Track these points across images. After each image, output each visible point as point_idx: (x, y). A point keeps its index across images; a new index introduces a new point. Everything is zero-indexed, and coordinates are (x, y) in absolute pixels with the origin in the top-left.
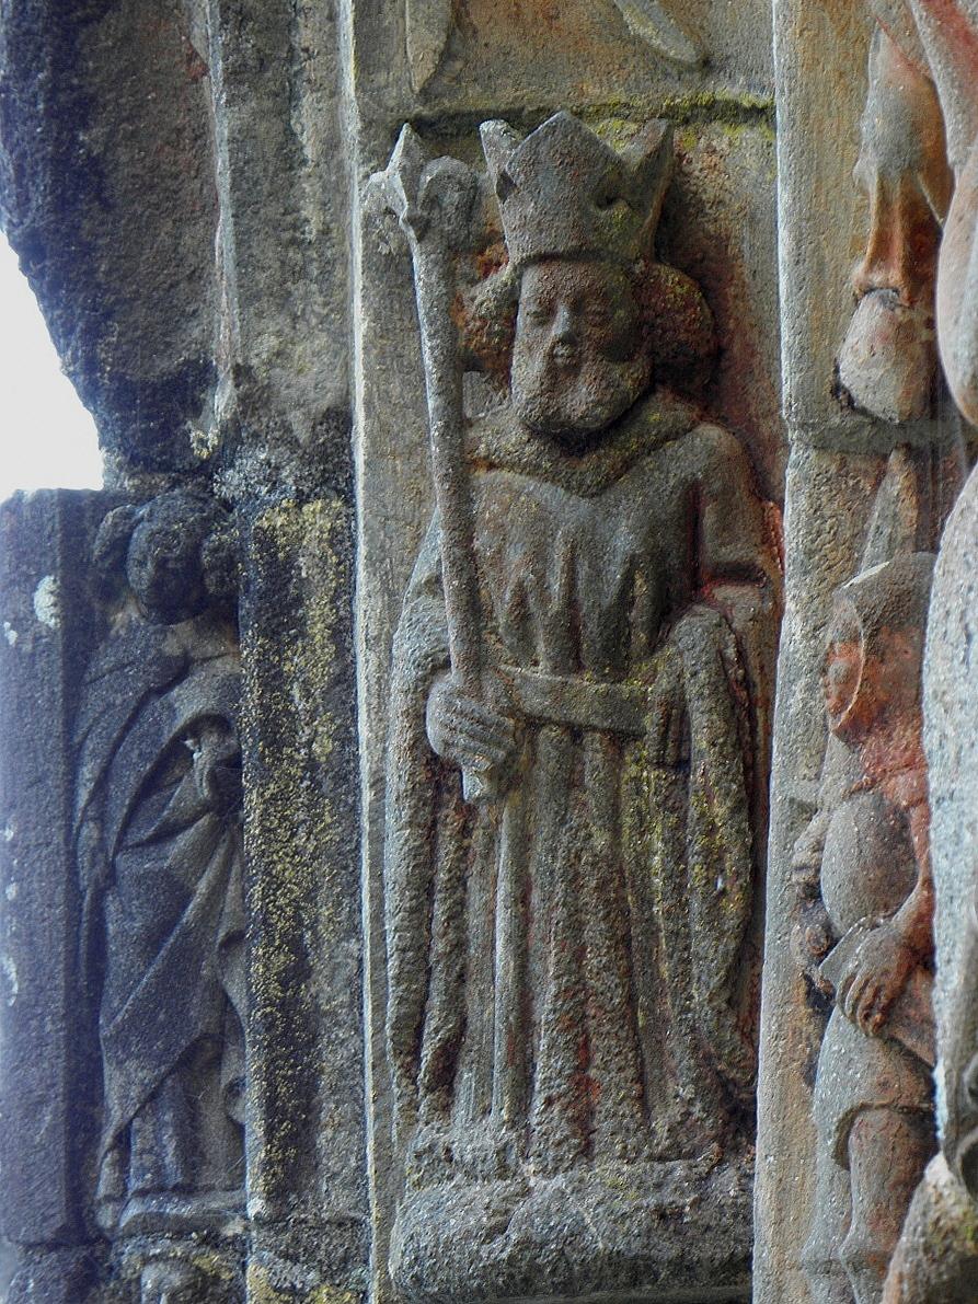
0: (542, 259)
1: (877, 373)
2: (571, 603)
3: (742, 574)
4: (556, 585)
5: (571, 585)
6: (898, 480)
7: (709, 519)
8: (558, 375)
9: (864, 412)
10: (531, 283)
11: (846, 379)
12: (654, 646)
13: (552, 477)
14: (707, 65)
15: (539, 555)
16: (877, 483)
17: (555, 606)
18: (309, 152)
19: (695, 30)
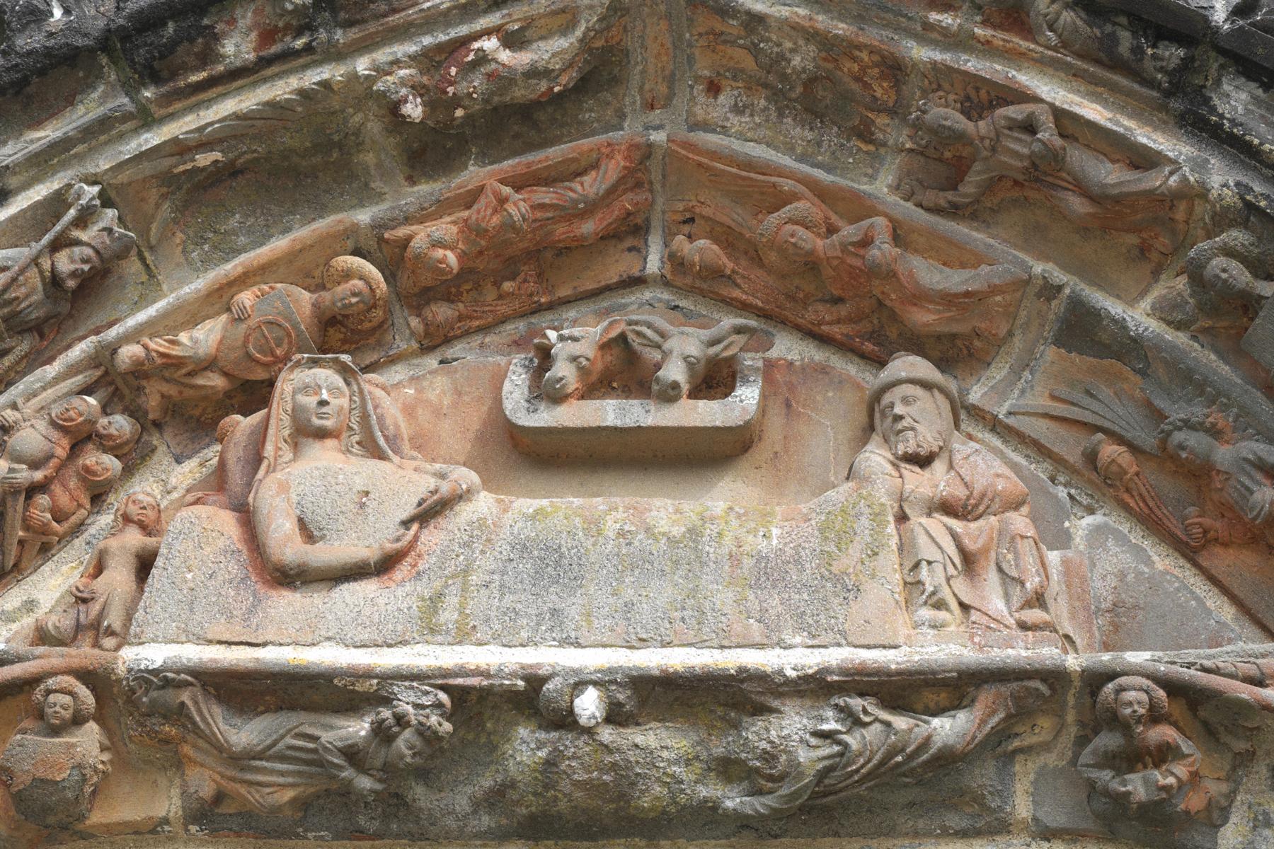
0: (97, 252)
1: (127, 360)
2: (21, 312)
3: (42, 336)
4: (23, 305)
5: (25, 309)
6: (98, 373)
7: (52, 321)
8: (73, 274)
9: (112, 358)
10: (89, 252)
11: (120, 350)
12: (19, 333)
13: (44, 284)
14: (151, 248)
15: (27, 296)
16: (95, 367)
17: (18, 309)
18: (72, 152)
19: (159, 241)
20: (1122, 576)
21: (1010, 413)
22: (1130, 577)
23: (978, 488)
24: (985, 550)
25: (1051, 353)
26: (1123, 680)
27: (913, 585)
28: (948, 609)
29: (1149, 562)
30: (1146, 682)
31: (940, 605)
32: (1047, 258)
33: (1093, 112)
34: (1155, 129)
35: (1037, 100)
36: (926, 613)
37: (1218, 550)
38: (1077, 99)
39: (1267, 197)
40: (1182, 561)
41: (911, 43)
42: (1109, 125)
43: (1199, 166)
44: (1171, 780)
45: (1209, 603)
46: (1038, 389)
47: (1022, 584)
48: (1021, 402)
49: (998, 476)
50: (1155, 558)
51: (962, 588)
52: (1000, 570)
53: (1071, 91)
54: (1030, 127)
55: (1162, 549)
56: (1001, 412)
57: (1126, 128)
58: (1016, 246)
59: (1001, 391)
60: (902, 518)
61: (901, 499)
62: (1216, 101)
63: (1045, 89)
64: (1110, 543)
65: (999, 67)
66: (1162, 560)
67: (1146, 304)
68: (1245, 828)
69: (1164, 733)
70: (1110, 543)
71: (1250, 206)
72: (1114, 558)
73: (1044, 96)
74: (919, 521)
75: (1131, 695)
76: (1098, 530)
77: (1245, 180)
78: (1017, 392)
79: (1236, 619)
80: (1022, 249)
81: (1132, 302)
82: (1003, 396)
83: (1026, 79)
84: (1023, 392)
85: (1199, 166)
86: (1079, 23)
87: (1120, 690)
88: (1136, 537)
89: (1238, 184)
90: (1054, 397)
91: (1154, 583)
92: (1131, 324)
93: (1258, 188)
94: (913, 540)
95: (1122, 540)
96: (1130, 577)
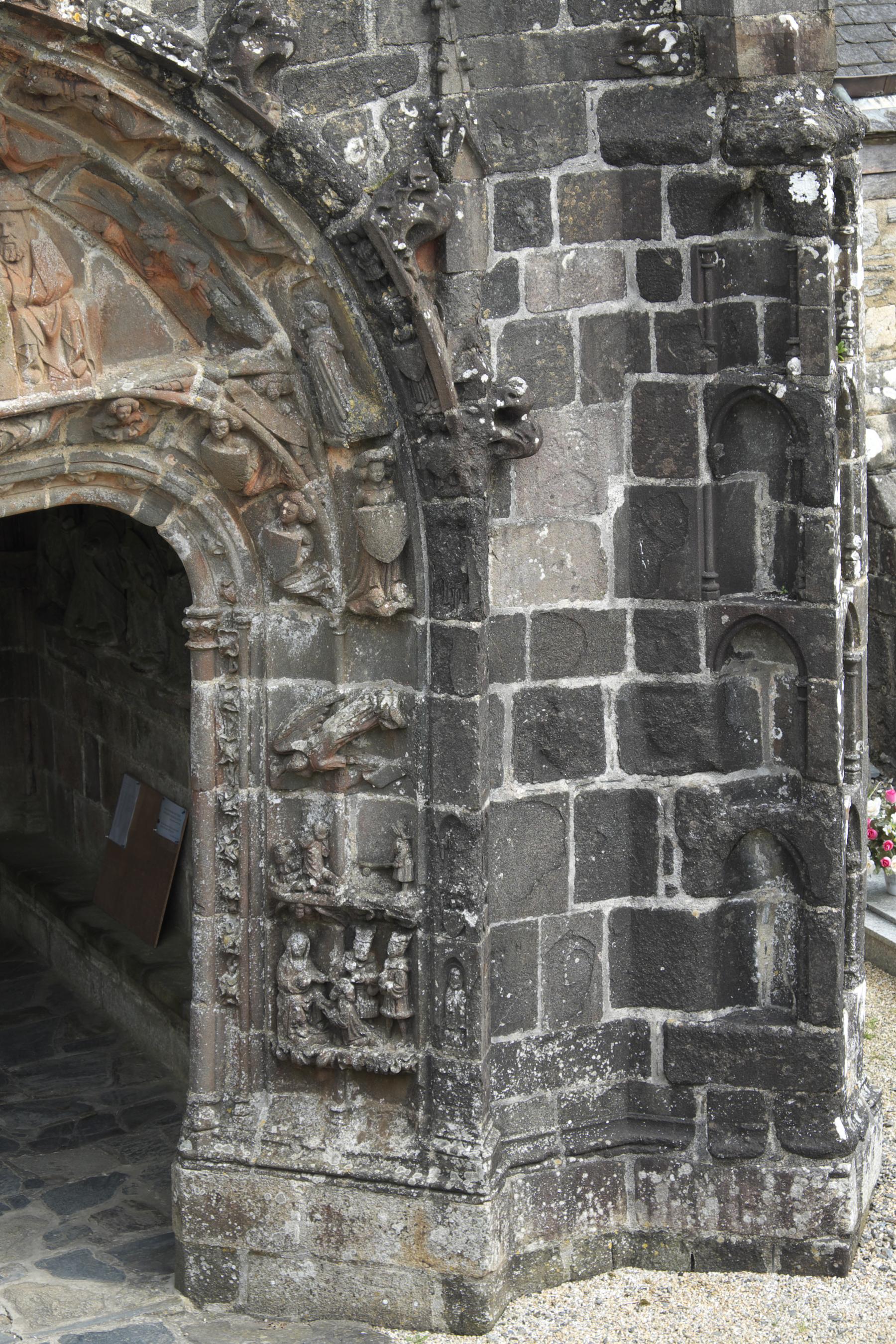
20: (109, 289)
21: (55, 200)
22: (113, 289)
23: (51, 288)
24: (56, 334)
25: (83, 171)
26: (121, 401)
27: (22, 358)
28: (39, 369)
29: (122, 279)
30: (131, 400)
31: (35, 367)
32: (87, 135)
33: (131, 95)
34: (163, 105)
35: (101, 86)
36: (29, 373)
37: (160, 278)
38: (123, 86)
39: (214, 147)
40: (139, 278)
41: (33, 49)
42: (139, 104)
43: (183, 129)
44: (135, 432)
45: (152, 303)
46: (72, 185)
47: (75, 350)
48: (63, 193)
49: (59, 274)
50: (126, 277)
51: (43, 349)
52: (62, 338)
53: (120, 80)
54: (96, 98)
55: (130, 270)
56: (51, 198)
57: (148, 106)
58: (73, 128)
59: (52, 186)
60: (12, 308)
61: (12, 298)
62: (196, 95)
63: (106, 80)
64: (104, 268)
65: (82, 66)
66: (130, 278)
67: (140, 164)
68: (162, 433)
69: (137, 416)
70: (104, 268)
71: (204, 151)
72: (106, 278)
73: (105, 85)
74: (24, 313)
75: (124, 409)
76: (98, 261)
77: (204, 136)
78: (60, 186)
79: (164, 312)
80: (79, 130)
81: (132, 162)
82: (53, 188)
83: (95, 72)
84: (64, 186)
85: (183, 129)
86: (132, 62)
87: (119, 406)
88: (118, 265)
89: (201, 139)
90: (80, 190)
91: (126, 291)
92: (131, 178)
93: (211, 142)
94: (21, 330)
95: (110, 266)
96: (113, 289)
